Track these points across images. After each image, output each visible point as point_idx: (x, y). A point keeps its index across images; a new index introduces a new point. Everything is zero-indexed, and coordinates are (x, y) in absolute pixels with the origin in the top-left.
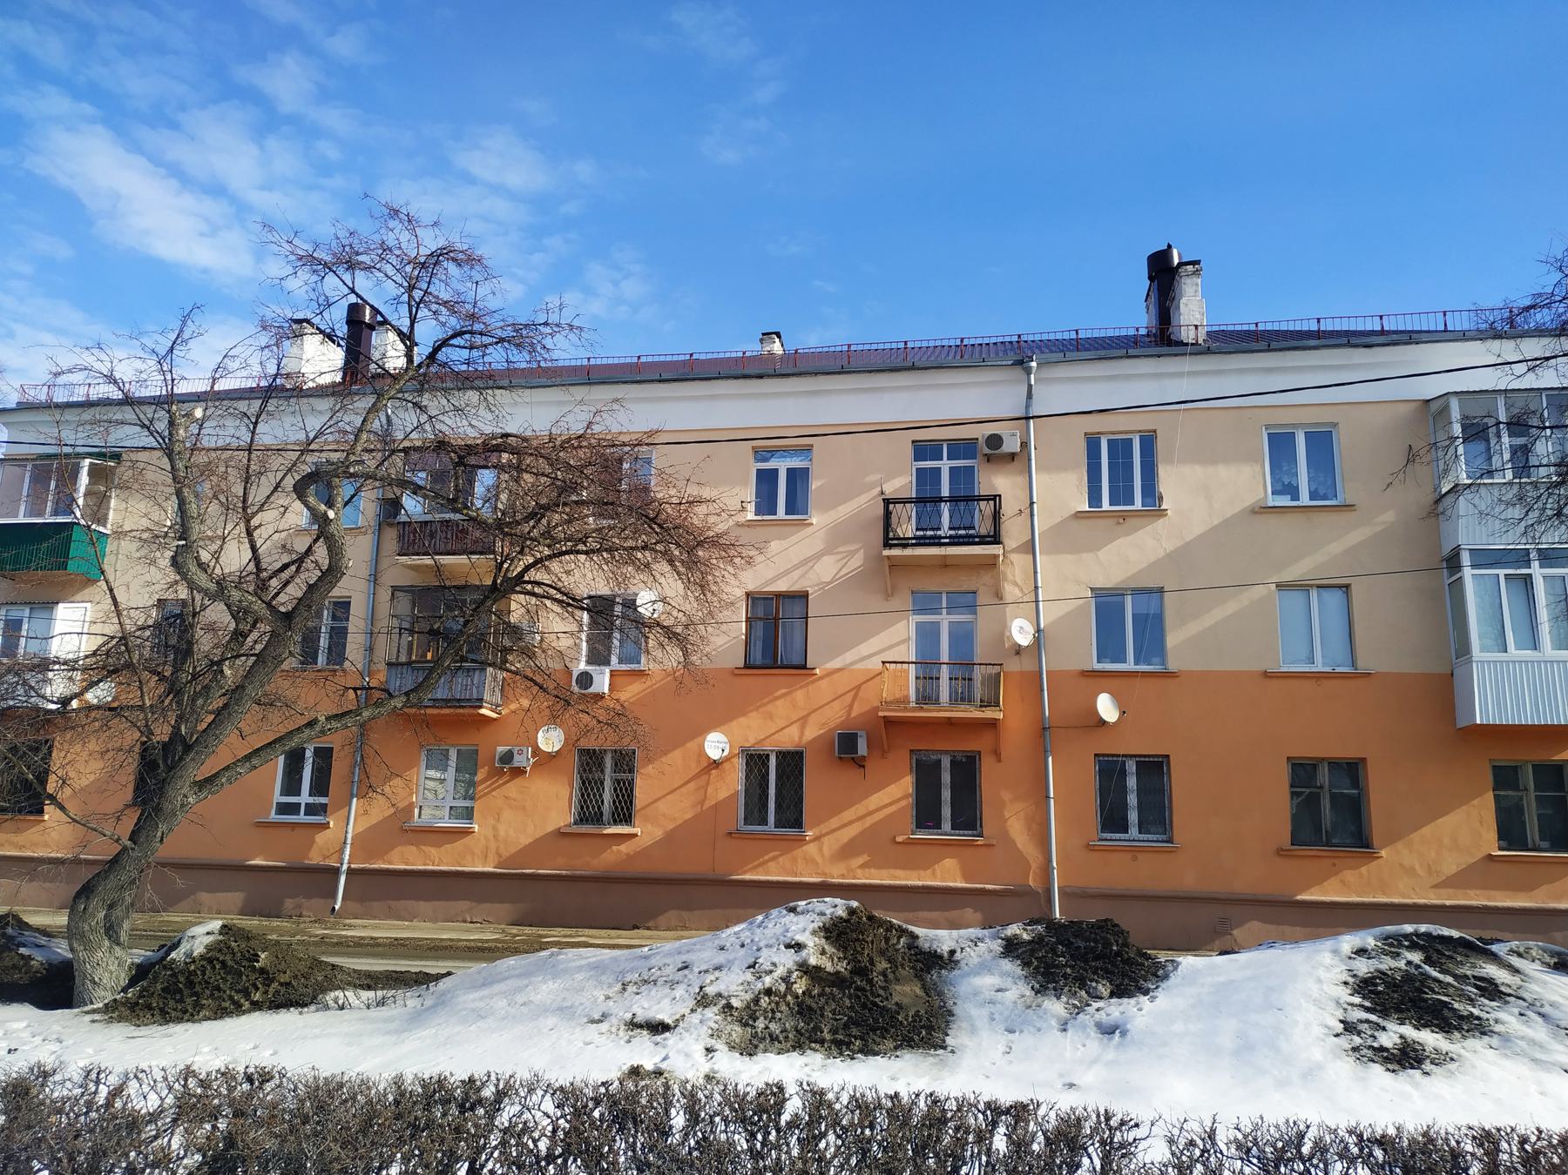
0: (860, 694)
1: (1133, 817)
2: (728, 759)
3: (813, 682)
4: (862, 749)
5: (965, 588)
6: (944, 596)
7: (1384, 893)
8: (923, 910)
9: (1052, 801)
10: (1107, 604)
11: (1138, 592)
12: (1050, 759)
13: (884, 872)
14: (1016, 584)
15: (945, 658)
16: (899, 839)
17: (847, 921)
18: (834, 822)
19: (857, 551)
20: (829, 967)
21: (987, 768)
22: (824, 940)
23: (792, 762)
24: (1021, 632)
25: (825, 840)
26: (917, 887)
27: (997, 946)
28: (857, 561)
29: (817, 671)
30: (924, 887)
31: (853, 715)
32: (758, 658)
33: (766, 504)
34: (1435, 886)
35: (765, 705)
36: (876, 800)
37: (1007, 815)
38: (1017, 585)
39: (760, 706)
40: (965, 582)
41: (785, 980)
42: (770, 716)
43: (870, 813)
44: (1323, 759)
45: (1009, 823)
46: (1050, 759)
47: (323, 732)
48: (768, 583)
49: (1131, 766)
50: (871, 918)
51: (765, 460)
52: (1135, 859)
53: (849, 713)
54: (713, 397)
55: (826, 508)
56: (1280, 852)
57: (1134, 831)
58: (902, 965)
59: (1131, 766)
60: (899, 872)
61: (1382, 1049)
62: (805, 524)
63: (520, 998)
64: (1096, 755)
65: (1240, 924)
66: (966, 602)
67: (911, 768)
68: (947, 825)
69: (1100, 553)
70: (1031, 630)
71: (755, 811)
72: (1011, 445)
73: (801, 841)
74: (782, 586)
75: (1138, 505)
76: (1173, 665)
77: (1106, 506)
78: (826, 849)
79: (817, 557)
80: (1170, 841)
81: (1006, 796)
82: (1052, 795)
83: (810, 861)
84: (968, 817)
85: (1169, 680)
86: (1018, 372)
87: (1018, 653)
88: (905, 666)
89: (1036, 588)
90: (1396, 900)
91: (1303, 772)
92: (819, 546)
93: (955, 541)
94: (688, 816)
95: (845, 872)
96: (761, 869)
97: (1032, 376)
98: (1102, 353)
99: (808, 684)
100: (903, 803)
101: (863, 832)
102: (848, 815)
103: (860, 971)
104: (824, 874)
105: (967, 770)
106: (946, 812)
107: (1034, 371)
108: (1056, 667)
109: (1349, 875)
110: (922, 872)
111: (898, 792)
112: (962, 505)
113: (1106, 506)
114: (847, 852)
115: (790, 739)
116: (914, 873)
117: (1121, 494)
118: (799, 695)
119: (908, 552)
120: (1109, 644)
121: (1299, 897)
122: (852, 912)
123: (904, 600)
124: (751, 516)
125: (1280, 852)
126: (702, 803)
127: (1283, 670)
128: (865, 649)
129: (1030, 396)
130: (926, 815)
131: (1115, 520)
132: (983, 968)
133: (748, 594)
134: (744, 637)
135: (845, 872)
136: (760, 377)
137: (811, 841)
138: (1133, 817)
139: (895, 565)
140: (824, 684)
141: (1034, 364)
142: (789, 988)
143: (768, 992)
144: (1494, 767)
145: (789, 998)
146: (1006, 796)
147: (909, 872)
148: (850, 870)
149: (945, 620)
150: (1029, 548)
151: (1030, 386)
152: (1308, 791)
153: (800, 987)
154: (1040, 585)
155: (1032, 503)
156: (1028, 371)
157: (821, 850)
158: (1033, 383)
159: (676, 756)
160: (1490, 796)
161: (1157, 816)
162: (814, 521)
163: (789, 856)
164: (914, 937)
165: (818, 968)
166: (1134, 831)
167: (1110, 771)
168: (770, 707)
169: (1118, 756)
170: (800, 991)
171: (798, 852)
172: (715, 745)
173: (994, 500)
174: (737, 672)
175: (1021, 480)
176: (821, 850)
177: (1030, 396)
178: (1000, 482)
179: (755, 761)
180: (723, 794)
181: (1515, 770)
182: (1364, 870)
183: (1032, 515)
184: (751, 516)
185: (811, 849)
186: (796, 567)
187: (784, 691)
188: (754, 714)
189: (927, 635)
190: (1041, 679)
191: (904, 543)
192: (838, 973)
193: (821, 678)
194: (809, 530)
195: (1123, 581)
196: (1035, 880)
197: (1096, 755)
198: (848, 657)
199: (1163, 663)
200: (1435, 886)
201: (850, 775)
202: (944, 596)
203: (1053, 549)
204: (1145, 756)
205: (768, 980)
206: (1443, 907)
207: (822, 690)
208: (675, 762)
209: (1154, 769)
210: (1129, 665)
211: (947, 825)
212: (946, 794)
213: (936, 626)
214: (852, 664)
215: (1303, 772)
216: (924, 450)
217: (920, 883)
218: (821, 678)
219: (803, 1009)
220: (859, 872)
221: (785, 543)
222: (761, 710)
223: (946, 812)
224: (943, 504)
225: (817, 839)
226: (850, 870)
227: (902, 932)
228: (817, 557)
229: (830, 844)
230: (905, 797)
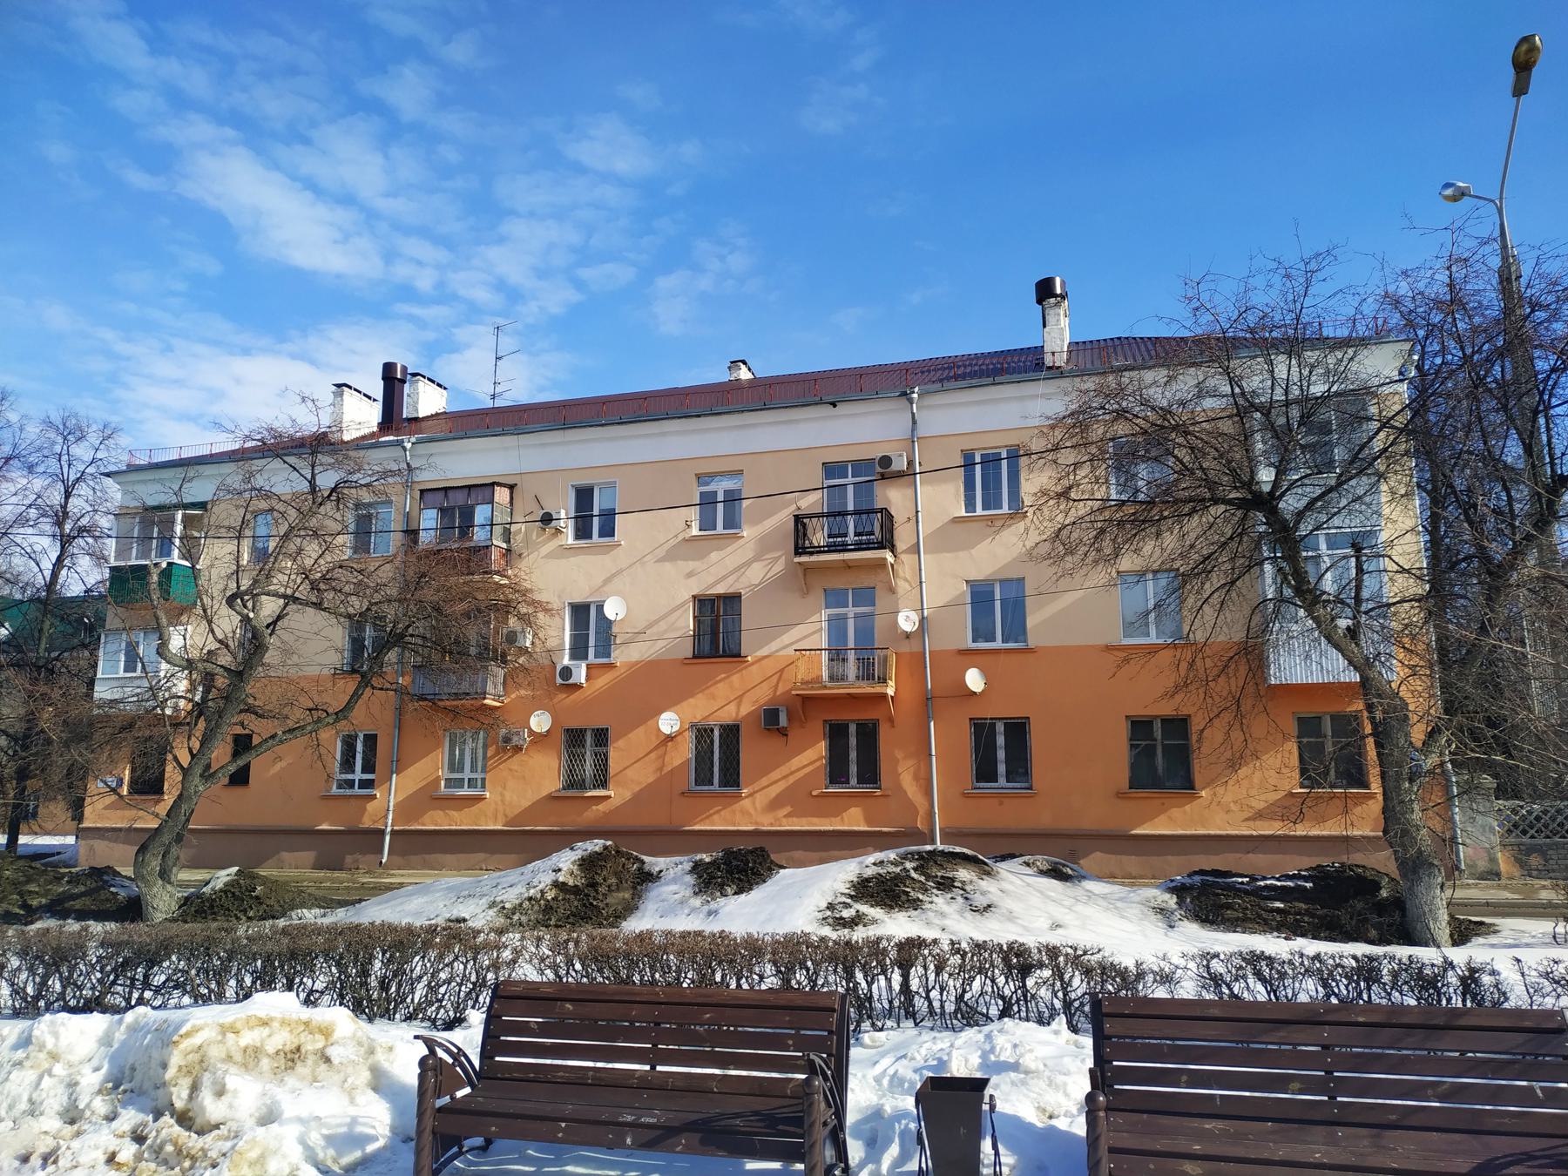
0: (784, 675)
1: (1002, 768)
2: (679, 733)
3: (746, 667)
4: (783, 721)
5: (866, 584)
6: (850, 592)
7: (1204, 827)
8: (797, 849)
9: (934, 758)
10: (980, 595)
11: (1004, 582)
12: (932, 724)
13: (804, 820)
14: (906, 580)
15: (851, 644)
16: (814, 793)
17: (600, 854)
18: (764, 781)
19: (780, 557)
20: (571, 883)
21: (884, 733)
22: (576, 867)
23: (731, 733)
24: (907, 621)
25: (757, 795)
26: (829, 831)
27: (688, 866)
28: (779, 567)
29: (749, 658)
30: (833, 831)
31: (778, 693)
32: (707, 648)
33: (707, 523)
34: (1247, 819)
35: (708, 688)
36: (797, 762)
37: (900, 770)
38: (907, 581)
39: (704, 690)
40: (866, 580)
41: (542, 892)
42: (713, 697)
43: (792, 773)
44: (1157, 716)
45: (901, 777)
46: (932, 724)
47: (281, 742)
48: (710, 587)
49: (1000, 727)
50: (617, 852)
51: (708, 484)
52: (1001, 804)
53: (775, 691)
54: (664, 434)
55: (755, 522)
56: (1120, 795)
57: (1002, 781)
58: (627, 881)
59: (1000, 727)
60: (815, 820)
61: (841, 918)
62: (737, 537)
63: (398, 909)
64: (971, 719)
65: (1086, 855)
66: (866, 596)
67: (825, 734)
68: (854, 781)
69: (973, 551)
70: (915, 617)
71: (703, 776)
72: (900, 464)
73: (738, 797)
74: (720, 589)
75: (1005, 509)
76: (1032, 643)
77: (979, 511)
78: (758, 805)
79: (748, 564)
80: (1030, 788)
81: (899, 754)
82: (934, 753)
83: (745, 812)
84: (870, 774)
85: (1031, 655)
86: (904, 401)
87: (908, 637)
88: (818, 652)
89: (921, 582)
90: (1212, 832)
91: (1140, 727)
92: (750, 555)
93: (859, 547)
94: (651, 780)
95: (773, 821)
96: (707, 821)
97: (914, 406)
98: (974, 382)
99: (742, 669)
100: (818, 764)
101: (787, 788)
102: (775, 775)
103: (593, 885)
104: (757, 823)
105: (869, 734)
106: (853, 769)
107: (915, 401)
108: (937, 648)
109: (1175, 812)
110: (833, 819)
111: (816, 753)
112: (839, 519)
113: (979, 511)
114: (775, 804)
115: (729, 715)
116: (827, 820)
117: (991, 501)
118: (735, 679)
119: (814, 558)
120: (982, 631)
121: (1133, 832)
122: (606, 848)
123: (818, 597)
124: (695, 531)
125: (1120, 795)
126: (661, 769)
127: (1123, 643)
128: (787, 638)
129: (914, 422)
130: (837, 773)
131: (985, 523)
132: (674, 881)
133: (694, 597)
134: (692, 633)
135: (773, 821)
136: (699, 416)
137: (746, 797)
138: (1002, 768)
139: (807, 569)
140: (754, 668)
141: (915, 396)
142: (542, 896)
143: (530, 899)
144: (1299, 719)
145: (542, 902)
146: (899, 754)
147: (822, 819)
148: (777, 820)
149: (851, 611)
150: (915, 549)
151: (913, 414)
152: (1144, 743)
153: (550, 896)
154: (923, 580)
155: (917, 512)
156: (911, 401)
157: (754, 803)
158: (915, 411)
159: (640, 731)
160: (1292, 747)
161: (1020, 766)
162: (745, 534)
163: (729, 809)
164: (643, 862)
165: (564, 884)
166: (1002, 781)
167: (982, 731)
168: (712, 689)
169: (986, 719)
170: (549, 898)
171: (737, 806)
172: (668, 722)
173: (881, 512)
174: (686, 661)
175: (910, 492)
176: (754, 803)
177: (914, 422)
178: (893, 497)
179: (703, 734)
180: (677, 762)
181: (1318, 719)
182: (1187, 808)
183: (917, 522)
184: (695, 531)
185: (746, 803)
186: (732, 573)
187: (723, 676)
188: (700, 695)
189: (837, 626)
190: (925, 658)
191: (819, 551)
192: (576, 886)
193: (752, 664)
194: (741, 542)
195: (989, 576)
196: (922, 823)
197: (971, 719)
198: (774, 646)
199: (1025, 641)
200: (1247, 819)
201: (776, 742)
202: (850, 592)
203: (934, 549)
204: (1011, 718)
205: (532, 892)
206: (1251, 837)
207: (753, 674)
208: (638, 736)
209: (1018, 730)
210: (998, 644)
211: (854, 781)
212: (853, 755)
213: (844, 618)
214: (777, 651)
215: (1140, 727)
216: (831, 469)
217: (831, 828)
218: (752, 664)
219: (548, 909)
220: (784, 820)
221: (722, 553)
222: (706, 692)
223: (853, 769)
224: (849, 517)
225: (751, 795)
226: (777, 820)
227: (637, 859)
228: (748, 564)
229: (761, 799)
230: (820, 758)
